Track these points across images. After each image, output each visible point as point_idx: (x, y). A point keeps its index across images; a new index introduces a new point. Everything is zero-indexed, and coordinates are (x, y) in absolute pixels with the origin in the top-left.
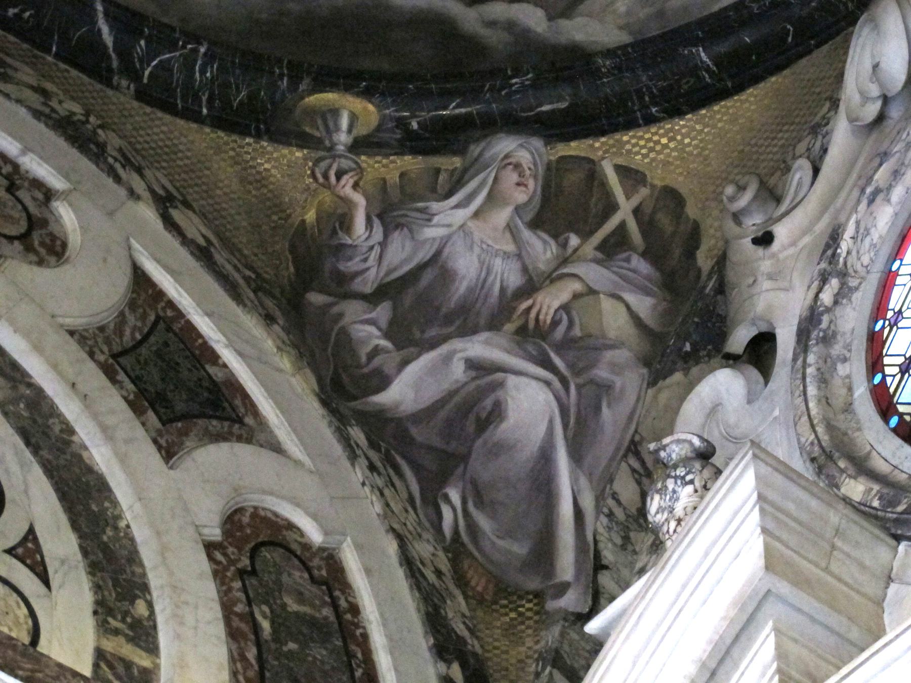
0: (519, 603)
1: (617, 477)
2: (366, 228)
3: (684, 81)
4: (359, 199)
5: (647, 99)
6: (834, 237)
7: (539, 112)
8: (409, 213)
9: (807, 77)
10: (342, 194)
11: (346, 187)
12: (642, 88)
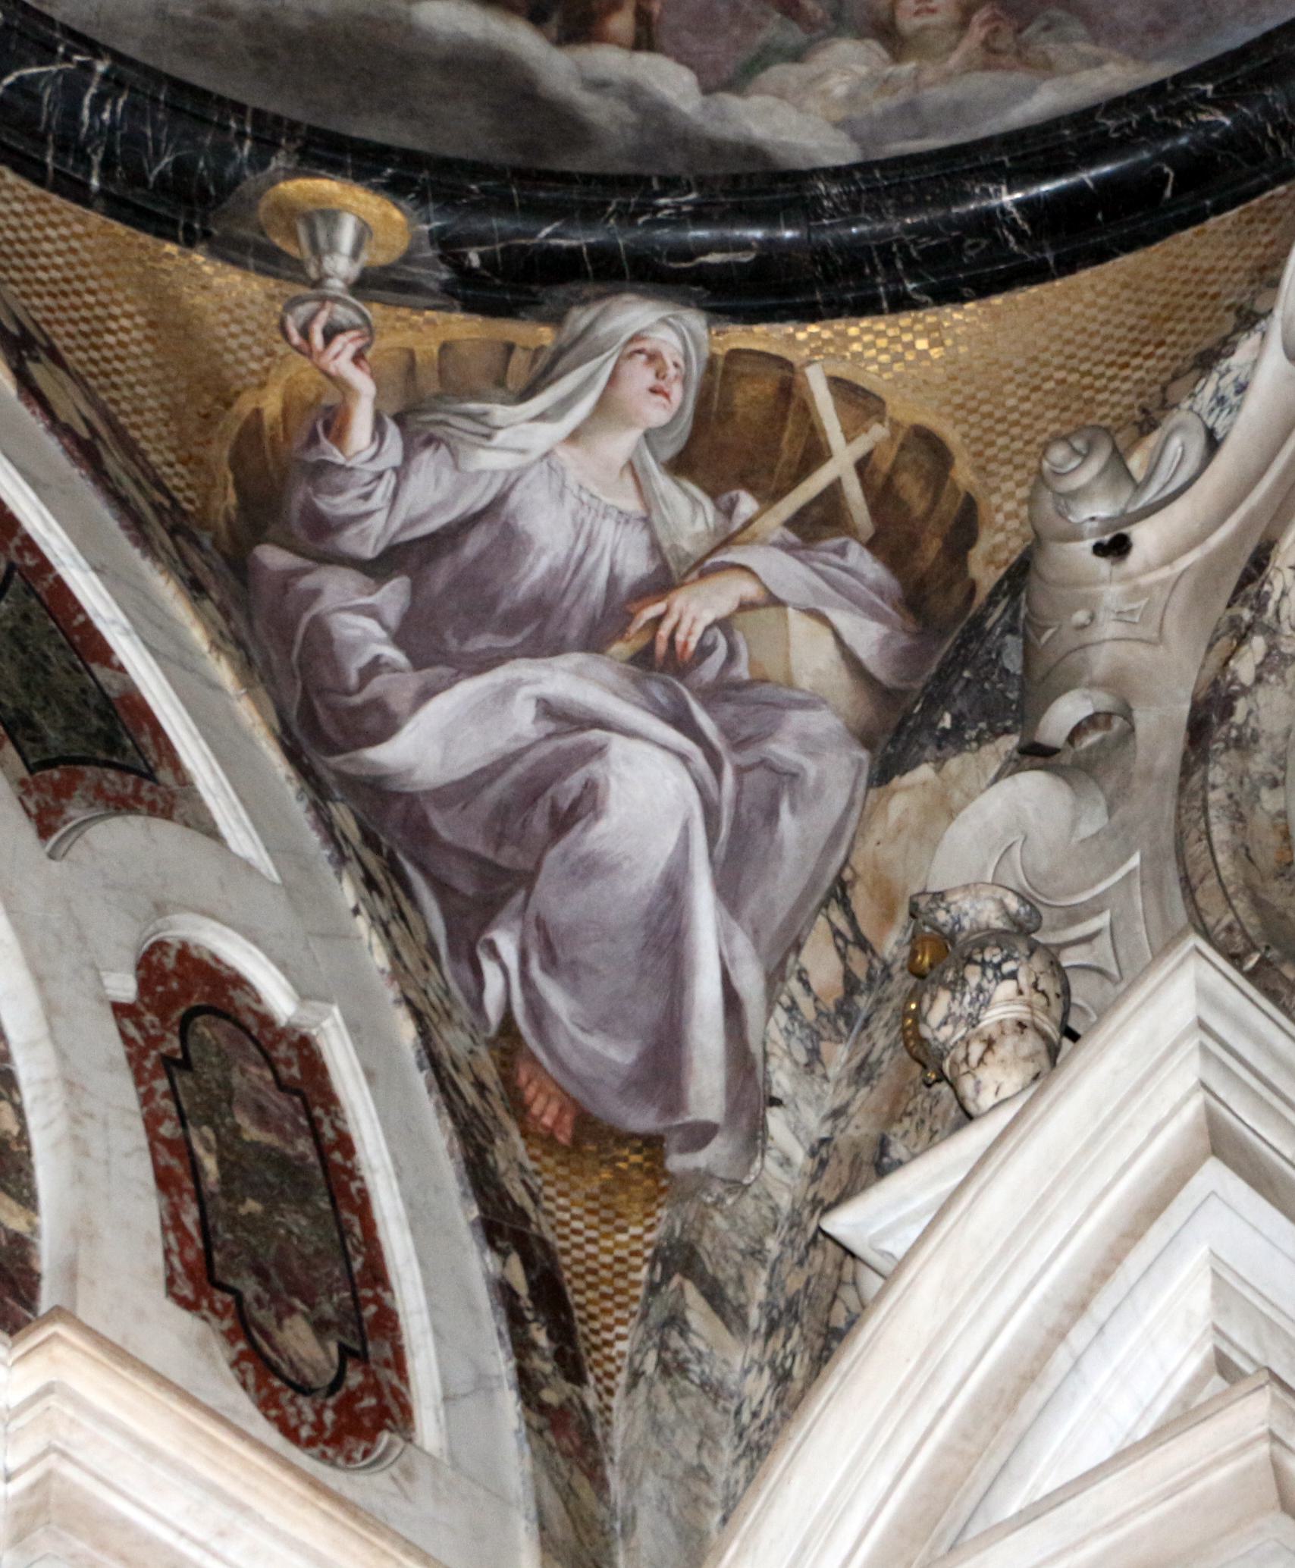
0: (616, 1152)
1: (809, 942)
2: (373, 439)
4: (363, 383)
5: (899, 265)
6: (1260, 561)
7: (701, 265)
8: (453, 420)
9: (1192, 264)
10: (332, 369)
11: (340, 357)
12: (889, 245)
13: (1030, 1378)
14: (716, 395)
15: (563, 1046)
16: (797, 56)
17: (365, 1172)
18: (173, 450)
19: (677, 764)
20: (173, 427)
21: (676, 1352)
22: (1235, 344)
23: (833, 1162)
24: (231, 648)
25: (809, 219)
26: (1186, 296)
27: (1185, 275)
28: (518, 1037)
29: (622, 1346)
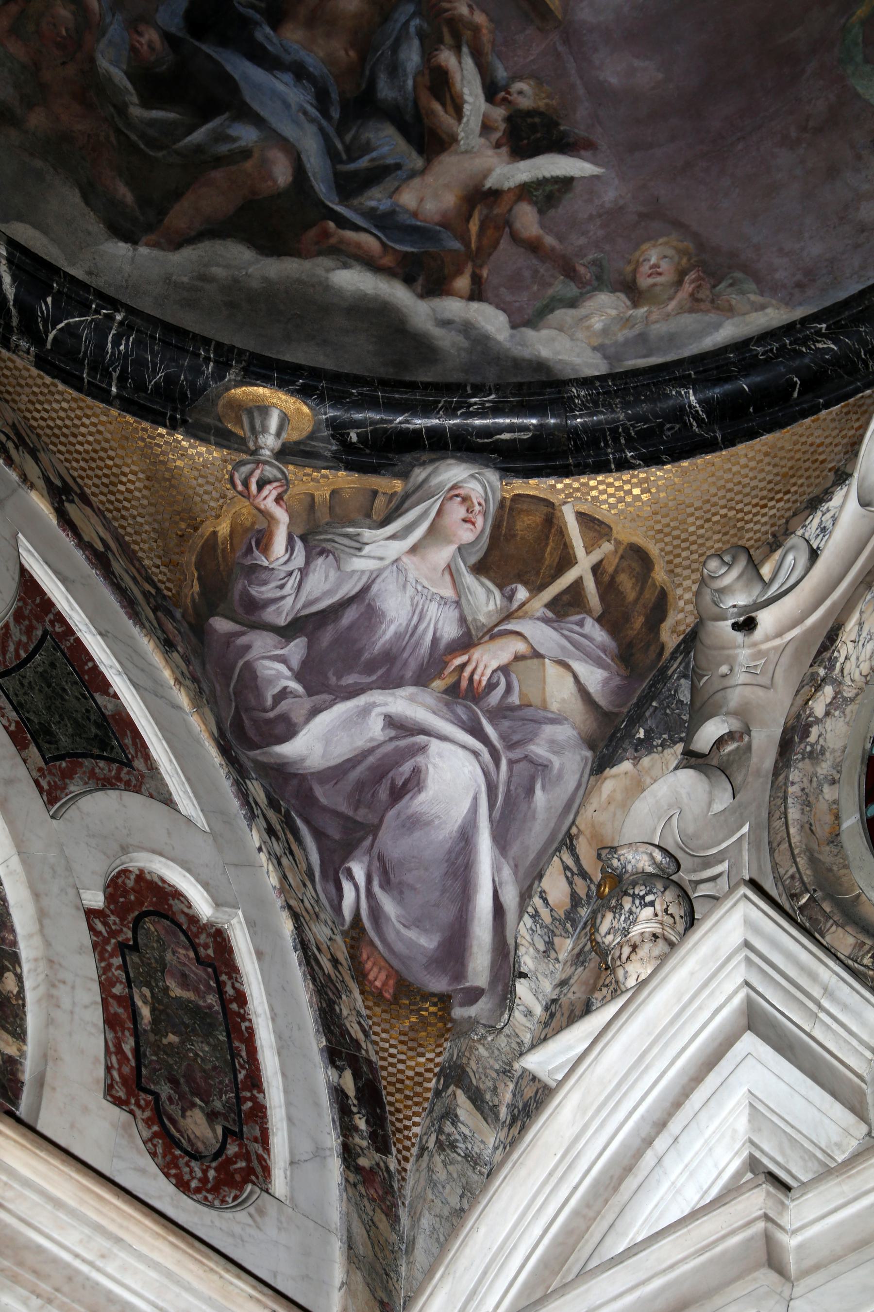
0: (421, 1005)
1: (547, 873)
2: (287, 551)
3: (668, 426)
4: (282, 515)
5: (623, 441)
6: (832, 636)
8: (337, 539)
9: (810, 441)
10: (262, 507)
12: (618, 427)
15: (391, 936)
16: (573, 304)
17: (252, 1017)
18: (159, 557)
19: (472, 758)
20: (160, 543)
21: (449, 1135)
22: (832, 493)
23: (558, 1015)
24: (188, 683)
25: (566, 411)
26: (805, 461)
27: (805, 448)
28: (363, 930)
29: (416, 1130)
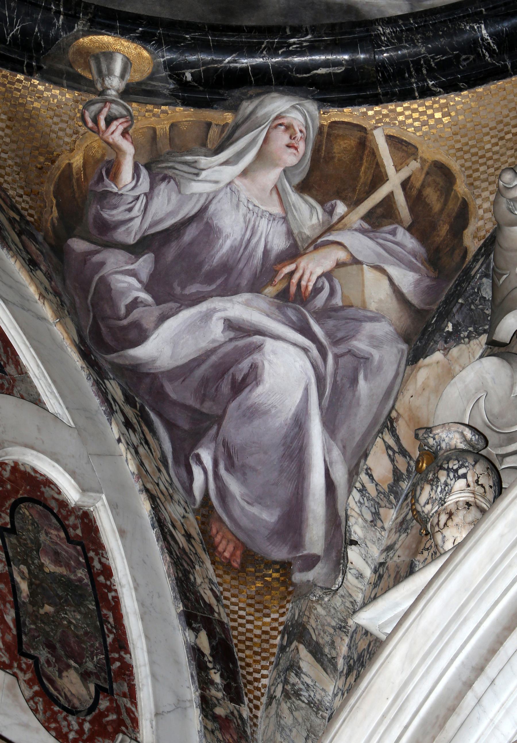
1: (372, 452)
2: (133, 178)
3: (464, 57)
5: (425, 72)
8: (177, 166)
10: (111, 140)
12: (420, 60)
13: (452, 710)
14: (324, 148)
15: (237, 512)
17: (118, 587)
18: (22, 188)
19: (302, 354)
20: (22, 175)
21: (294, 685)
23: (386, 576)
24: (51, 297)
25: (374, 47)
28: (212, 507)
29: (265, 681)
